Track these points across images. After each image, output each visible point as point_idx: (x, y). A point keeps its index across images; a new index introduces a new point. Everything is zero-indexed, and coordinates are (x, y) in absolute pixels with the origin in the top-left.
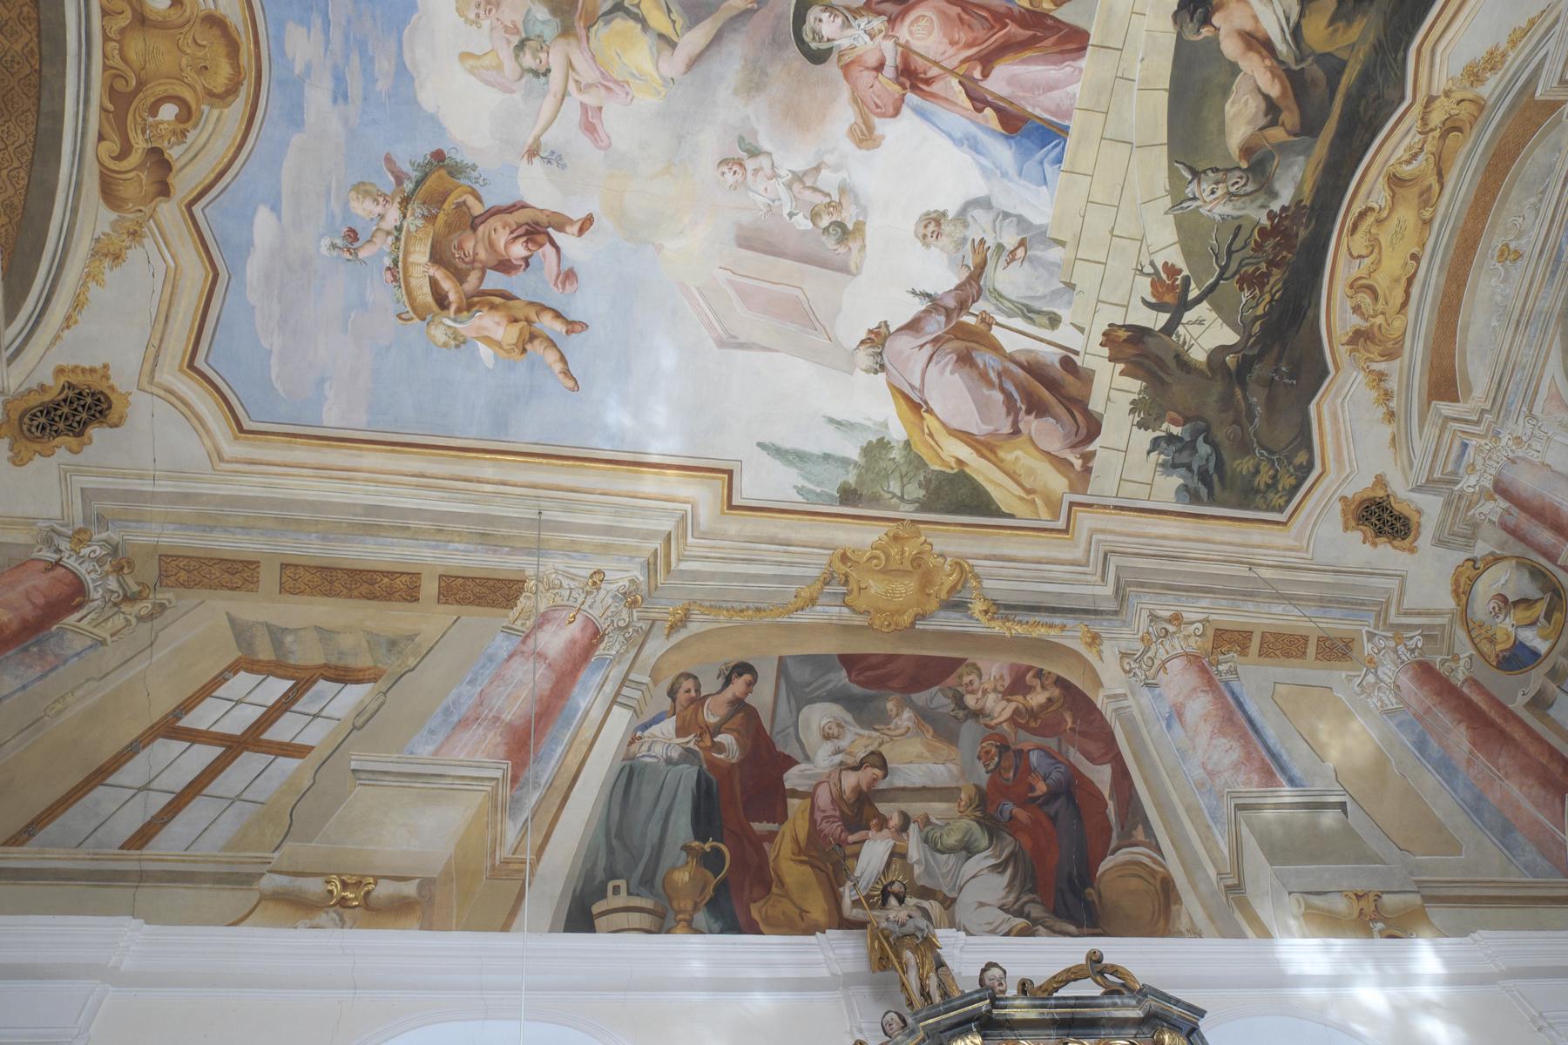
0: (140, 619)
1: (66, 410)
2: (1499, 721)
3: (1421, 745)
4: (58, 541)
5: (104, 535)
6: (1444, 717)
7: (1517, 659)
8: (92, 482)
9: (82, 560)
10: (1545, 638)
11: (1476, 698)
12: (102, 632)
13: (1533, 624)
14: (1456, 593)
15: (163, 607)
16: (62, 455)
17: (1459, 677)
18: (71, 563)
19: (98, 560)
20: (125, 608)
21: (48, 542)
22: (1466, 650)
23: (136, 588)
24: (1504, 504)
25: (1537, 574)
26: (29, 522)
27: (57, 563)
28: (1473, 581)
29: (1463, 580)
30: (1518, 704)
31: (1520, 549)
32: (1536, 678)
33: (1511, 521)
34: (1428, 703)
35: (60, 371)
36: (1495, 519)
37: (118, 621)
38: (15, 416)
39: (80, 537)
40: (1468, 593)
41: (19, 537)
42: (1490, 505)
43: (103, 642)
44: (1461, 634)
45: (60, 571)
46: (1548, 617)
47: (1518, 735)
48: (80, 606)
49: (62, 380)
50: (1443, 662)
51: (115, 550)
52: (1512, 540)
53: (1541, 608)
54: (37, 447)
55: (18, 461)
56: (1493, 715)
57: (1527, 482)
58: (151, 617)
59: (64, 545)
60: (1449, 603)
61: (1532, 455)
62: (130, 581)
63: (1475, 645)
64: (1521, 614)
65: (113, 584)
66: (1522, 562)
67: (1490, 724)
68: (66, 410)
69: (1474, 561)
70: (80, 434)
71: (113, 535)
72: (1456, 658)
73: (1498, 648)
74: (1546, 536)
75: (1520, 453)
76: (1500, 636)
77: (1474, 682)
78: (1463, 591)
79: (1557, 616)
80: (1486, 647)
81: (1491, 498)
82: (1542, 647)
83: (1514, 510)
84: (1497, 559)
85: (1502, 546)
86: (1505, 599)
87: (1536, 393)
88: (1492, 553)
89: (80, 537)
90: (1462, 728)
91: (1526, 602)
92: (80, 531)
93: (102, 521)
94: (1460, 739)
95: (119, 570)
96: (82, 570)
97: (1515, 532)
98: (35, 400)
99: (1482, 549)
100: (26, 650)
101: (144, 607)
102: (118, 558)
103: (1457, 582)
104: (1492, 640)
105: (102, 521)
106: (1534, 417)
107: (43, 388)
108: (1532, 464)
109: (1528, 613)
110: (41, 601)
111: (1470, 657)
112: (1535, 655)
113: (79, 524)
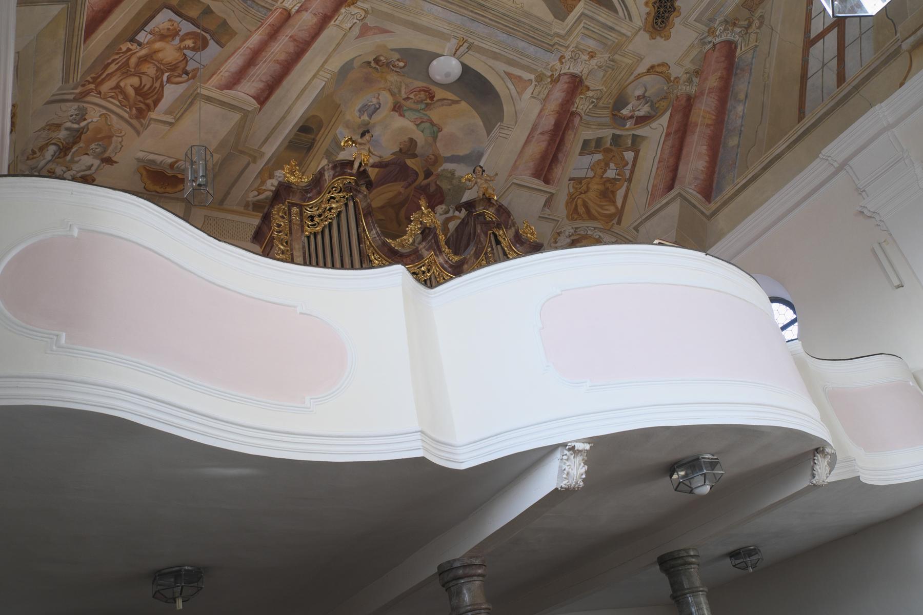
0: (759, 28)
1: (662, 10)
4: (706, 41)
5: (717, 22)
8: (695, 15)
9: (720, 35)
12: (752, 44)
15: (762, 17)
16: (677, 21)
18: (718, 40)
19: (725, 30)
20: (750, 31)
21: (704, 44)
23: (746, 22)
26: (692, 46)
27: (714, 45)
35: (646, 4)
37: (753, 36)
38: (651, 29)
39: (711, 32)
41: (695, 52)
43: (756, 46)
45: (717, 46)
48: (736, 47)
49: (651, 5)
51: (726, 22)
54: (667, 28)
55: (667, 38)
58: (762, 23)
59: (709, 39)
62: (742, 23)
65: (738, 30)
68: (662, 10)
70: (675, 9)
71: (720, 19)
89: (711, 32)
92: (709, 31)
93: (712, 20)
95: (734, 25)
96: (724, 38)
98: (651, 18)
100: (736, 74)
101: (756, 23)
102: (731, 23)
105: (712, 20)
107: (648, 14)
110: (723, 59)
113: (706, 29)
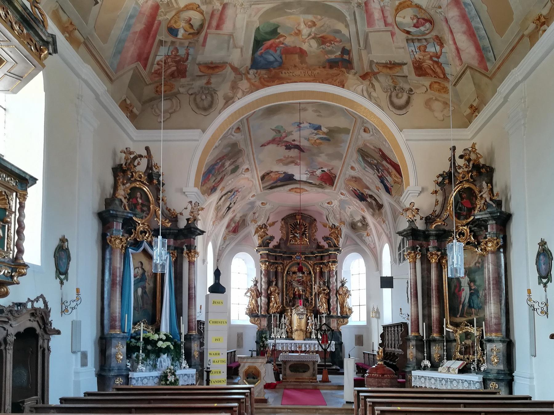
2: (151, 35)
3: (131, 17)
6: (144, 20)
7: (173, 31)
10: (183, 36)
11: (155, 26)
13: (185, 31)
14: (186, 6)
17: (159, 18)
22: (169, 16)
24: (220, 8)
25: (202, 26)
28: (193, 9)
29: (191, 6)
30: (158, 38)
31: (208, 19)
32: (171, 39)
33: (215, 12)
34: (147, 13)
36: (215, 8)
40: (188, 9)
42: (219, 5)
44: (173, 13)
46: (190, 34)
47: (150, 41)
50: (162, 12)
52: (210, 15)
53: (191, 31)
56: (152, 33)
57: (230, 12)
60: (182, 5)
61: (238, 11)
63: (172, 18)
64: (187, 27)
66: (204, 21)
67: (149, 33)
69: (199, 7)
72: (165, 15)
73: (175, 26)
74: (214, 23)
75: (238, 7)
76: (178, 24)
77: (160, 23)
78: (188, 7)
79: (191, 36)
80: (173, 22)
81: (221, 4)
82: (180, 36)
83: (219, 12)
84: (202, 13)
85: (207, 13)
86: (190, 20)
87: (258, 4)
88: (203, 11)
90: (144, 26)
91: (192, 26)
94: (139, 27)
97: (212, 14)
99: (203, 8)
103: (190, 5)
104: (176, 22)
106: (251, 6)
108: (236, 10)
109: (188, 28)
111: (167, 19)
112: (176, 35)
